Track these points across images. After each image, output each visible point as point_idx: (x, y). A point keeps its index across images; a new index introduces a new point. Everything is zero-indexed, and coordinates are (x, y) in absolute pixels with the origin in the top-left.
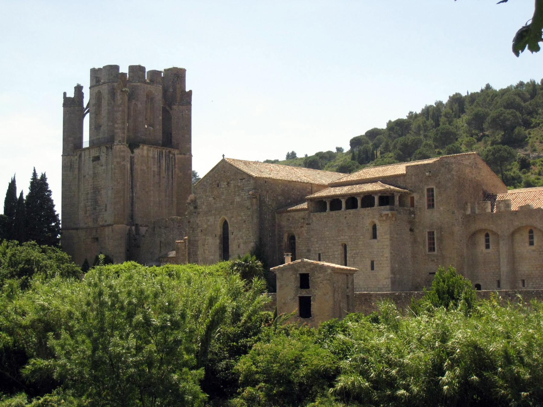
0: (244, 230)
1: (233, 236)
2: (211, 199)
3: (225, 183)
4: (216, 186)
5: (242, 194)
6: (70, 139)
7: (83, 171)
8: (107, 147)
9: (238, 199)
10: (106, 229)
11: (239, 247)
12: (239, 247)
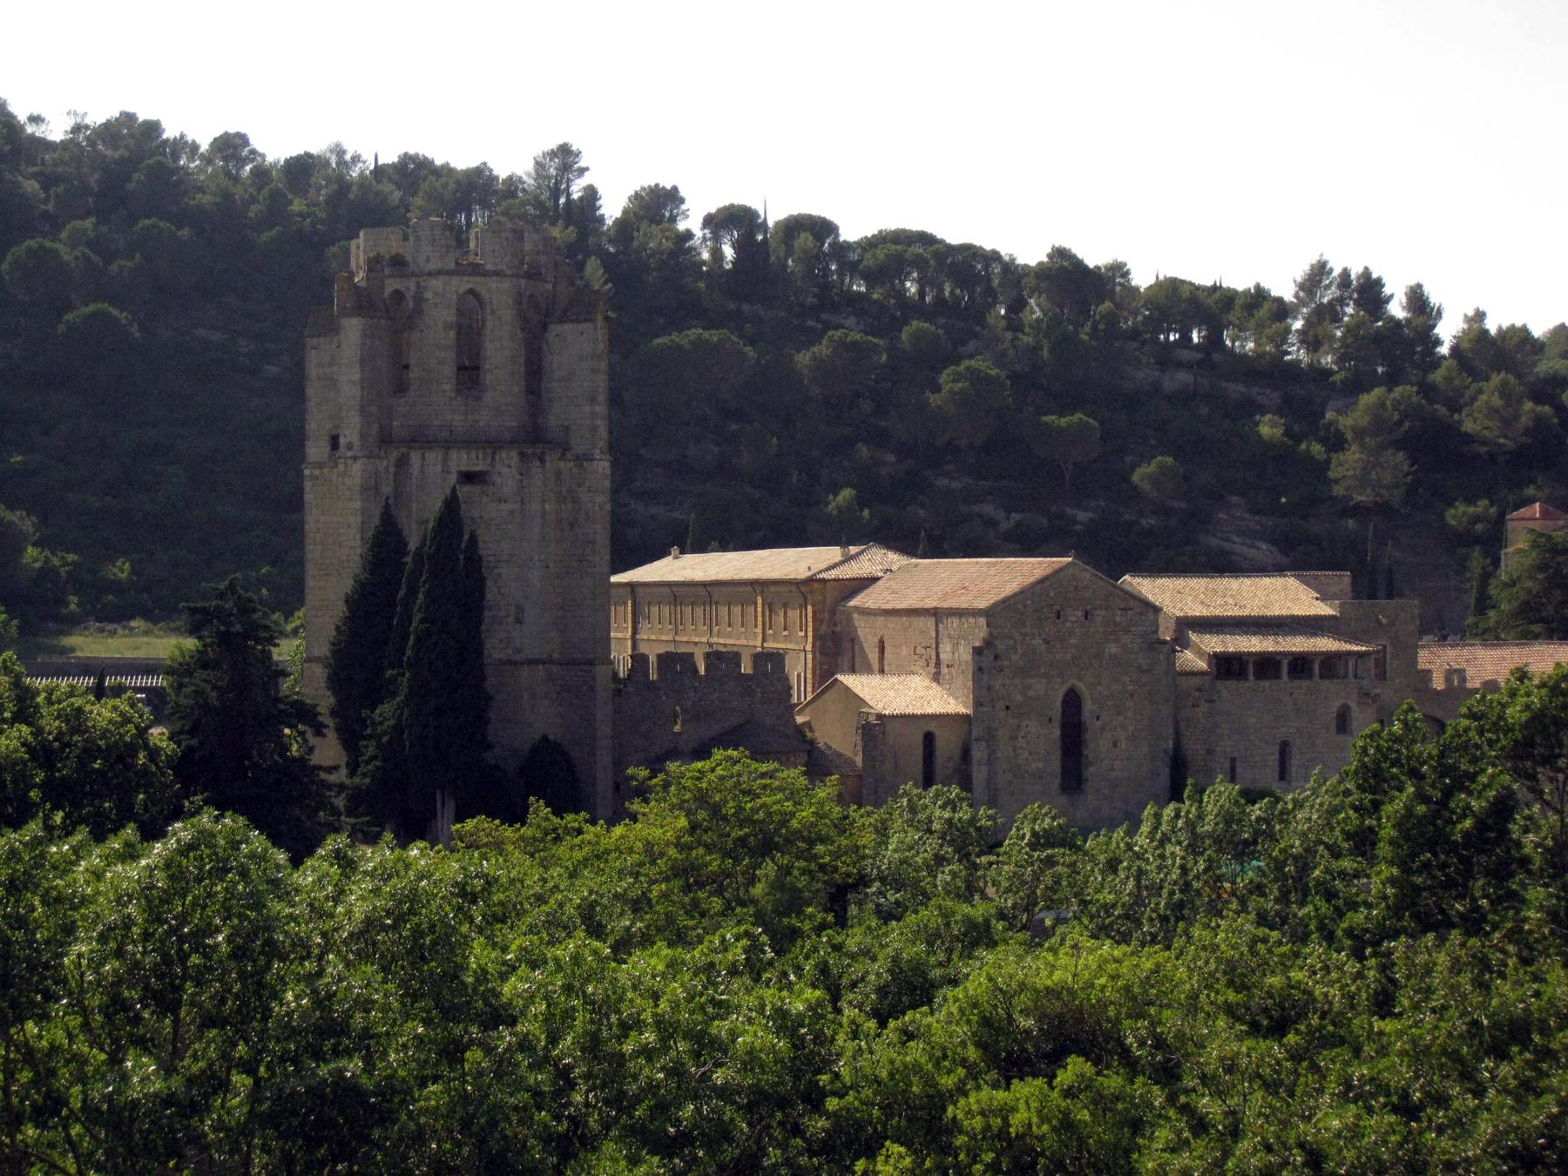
0: (1130, 714)
1: (1098, 724)
2: (1037, 641)
3: (1080, 613)
4: (1053, 616)
5: (1126, 639)
6: (374, 409)
7: (414, 506)
8: (522, 455)
9: (1113, 649)
10: (525, 672)
11: (1115, 745)
12: (1115, 745)
